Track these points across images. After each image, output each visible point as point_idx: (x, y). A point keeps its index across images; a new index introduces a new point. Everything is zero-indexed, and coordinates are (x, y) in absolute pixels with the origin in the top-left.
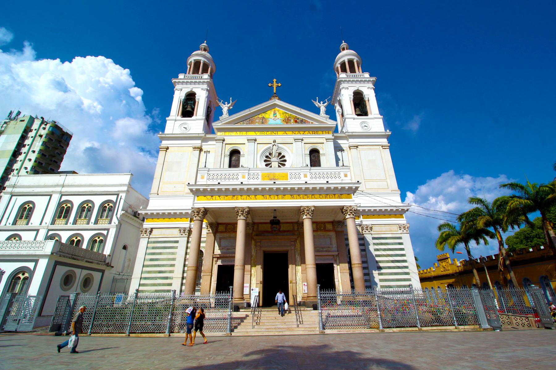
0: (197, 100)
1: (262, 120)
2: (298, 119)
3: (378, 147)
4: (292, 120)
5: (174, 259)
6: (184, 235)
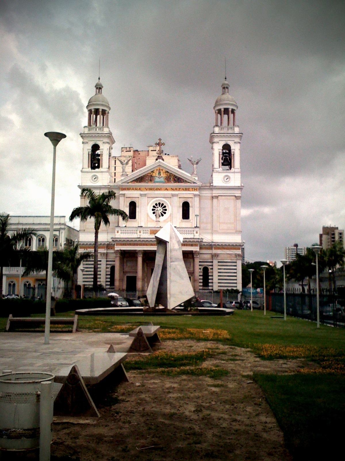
2: (176, 177)
3: (233, 197)
4: (172, 178)
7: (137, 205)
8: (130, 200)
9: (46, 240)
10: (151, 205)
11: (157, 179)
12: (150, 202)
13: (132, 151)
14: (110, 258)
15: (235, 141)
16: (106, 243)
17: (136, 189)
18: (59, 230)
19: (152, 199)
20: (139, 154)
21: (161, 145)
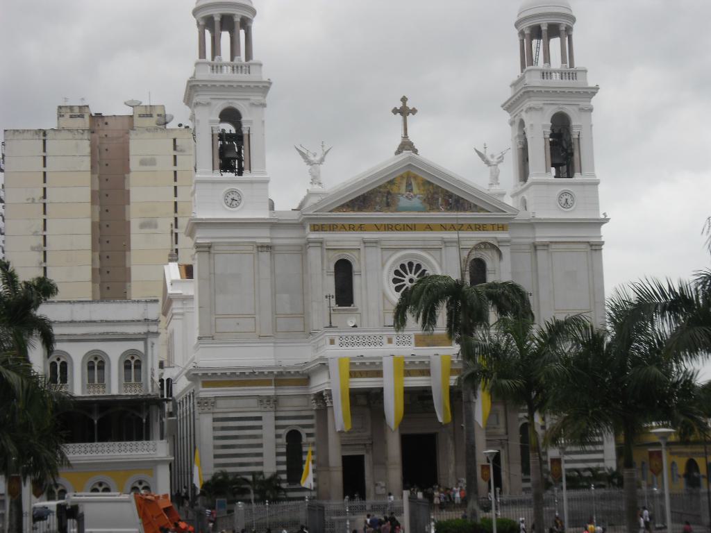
0: (245, 132)
1: (387, 199)
2: (451, 195)
3: (583, 246)
4: (440, 199)
5: (260, 446)
6: (269, 408)
7: (355, 268)
8: (335, 257)
9: (110, 365)
10: (391, 267)
11: (403, 202)
12: (386, 261)
13: (87, 117)
14: (282, 409)
15: (581, 107)
16: (275, 371)
17: (352, 228)
18: (144, 338)
19: (391, 252)
20: (106, 124)
21: (408, 114)
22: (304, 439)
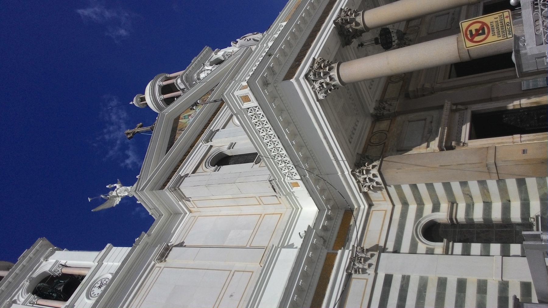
6: (373, 261)
22: (442, 216)
